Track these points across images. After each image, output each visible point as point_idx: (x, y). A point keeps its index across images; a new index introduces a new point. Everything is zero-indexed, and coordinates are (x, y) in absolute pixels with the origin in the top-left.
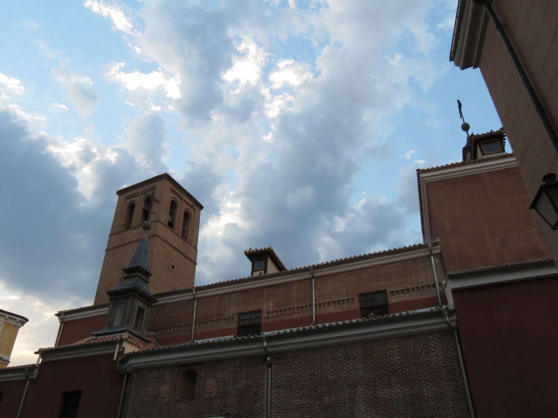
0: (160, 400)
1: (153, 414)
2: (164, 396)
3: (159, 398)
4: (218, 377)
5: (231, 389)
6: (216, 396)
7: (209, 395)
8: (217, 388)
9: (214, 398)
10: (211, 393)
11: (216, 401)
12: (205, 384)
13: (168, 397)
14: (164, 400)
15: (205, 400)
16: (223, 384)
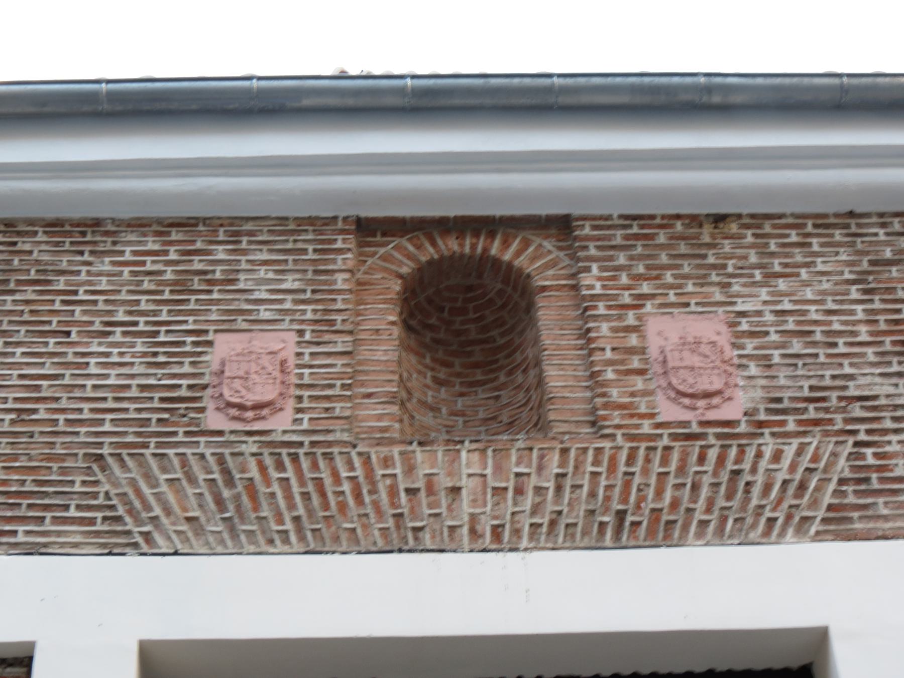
0: (214, 420)
1: (157, 511)
2: (251, 398)
3: (202, 410)
4: (739, 308)
5: (878, 380)
6: (762, 417)
7: (694, 408)
8: (753, 370)
9: (743, 428)
10: (708, 395)
11: (768, 452)
12: (633, 340)
13: (299, 411)
14: (257, 426)
15: (665, 441)
16: (797, 347)
